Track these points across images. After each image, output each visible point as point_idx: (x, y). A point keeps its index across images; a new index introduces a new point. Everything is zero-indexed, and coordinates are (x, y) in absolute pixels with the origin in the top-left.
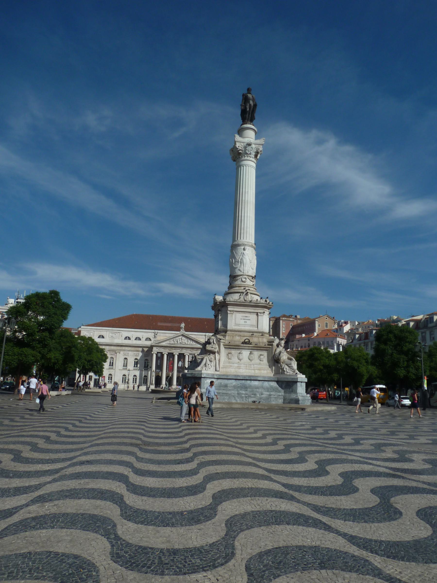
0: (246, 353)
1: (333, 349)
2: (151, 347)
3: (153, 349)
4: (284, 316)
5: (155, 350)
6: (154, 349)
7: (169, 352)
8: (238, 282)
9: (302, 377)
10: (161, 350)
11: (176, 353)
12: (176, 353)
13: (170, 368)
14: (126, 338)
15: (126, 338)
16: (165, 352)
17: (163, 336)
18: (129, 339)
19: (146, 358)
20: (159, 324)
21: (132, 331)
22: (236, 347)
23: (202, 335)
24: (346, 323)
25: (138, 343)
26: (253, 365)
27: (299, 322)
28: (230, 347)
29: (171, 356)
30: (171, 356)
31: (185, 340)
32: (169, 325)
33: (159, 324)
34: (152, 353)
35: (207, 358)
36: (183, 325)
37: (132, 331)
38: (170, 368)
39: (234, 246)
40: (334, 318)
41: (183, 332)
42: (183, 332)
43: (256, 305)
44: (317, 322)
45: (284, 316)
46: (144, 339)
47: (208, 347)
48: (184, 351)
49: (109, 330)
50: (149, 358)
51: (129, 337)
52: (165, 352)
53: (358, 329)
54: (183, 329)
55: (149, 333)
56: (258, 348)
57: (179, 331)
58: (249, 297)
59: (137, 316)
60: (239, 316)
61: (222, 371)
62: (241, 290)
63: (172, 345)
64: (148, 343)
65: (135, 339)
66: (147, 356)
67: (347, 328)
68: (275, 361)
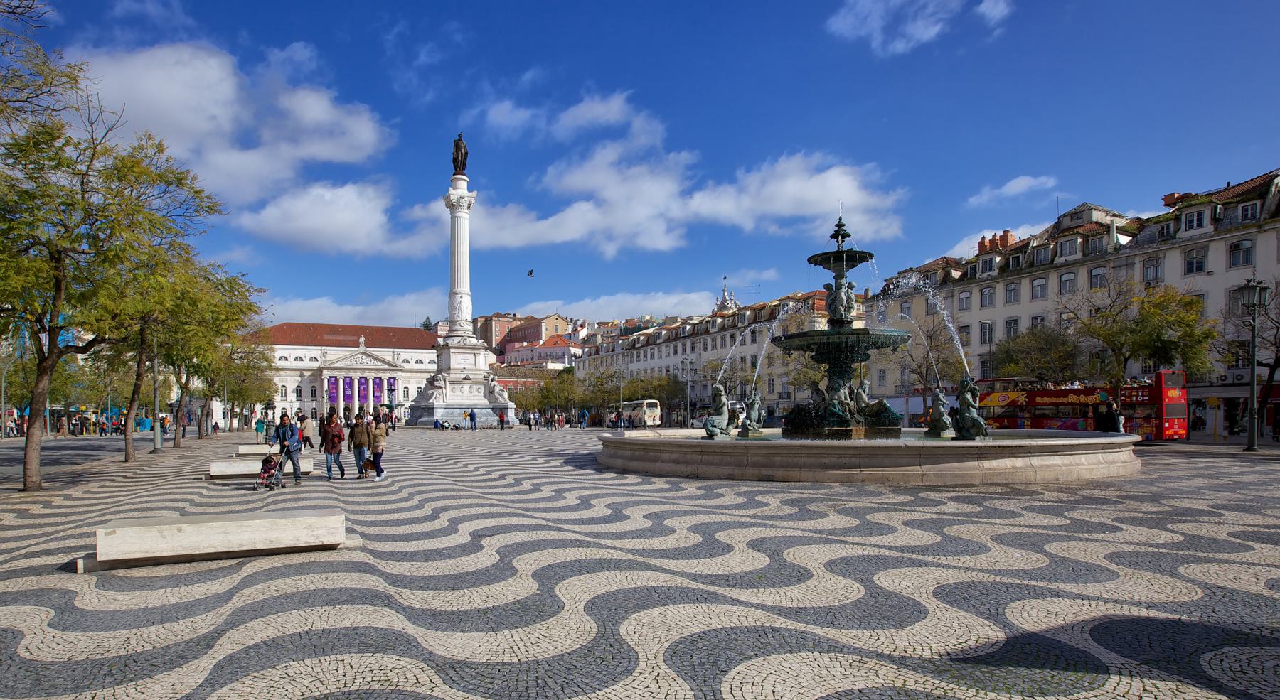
0: (466, 387)
2: (320, 370)
4: (498, 315)
5: (326, 374)
6: (325, 372)
8: (457, 327)
9: (512, 405)
10: (335, 374)
11: (356, 376)
12: (356, 376)
13: (348, 398)
15: (281, 359)
17: (336, 356)
20: (326, 337)
22: (459, 383)
24: (582, 326)
25: (299, 364)
26: (474, 398)
27: (519, 323)
28: (452, 383)
29: (349, 383)
30: (349, 383)
32: (341, 338)
33: (326, 337)
35: (436, 392)
36: (362, 339)
38: (348, 398)
39: (452, 294)
41: (362, 348)
42: (362, 348)
43: (474, 347)
45: (498, 315)
47: (436, 384)
48: (365, 374)
53: (596, 335)
55: (315, 351)
56: (477, 383)
57: (357, 345)
58: (467, 342)
59: (289, 325)
60: (460, 356)
61: (449, 401)
62: (461, 333)
64: (315, 365)
67: (583, 333)
68: (490, 393)
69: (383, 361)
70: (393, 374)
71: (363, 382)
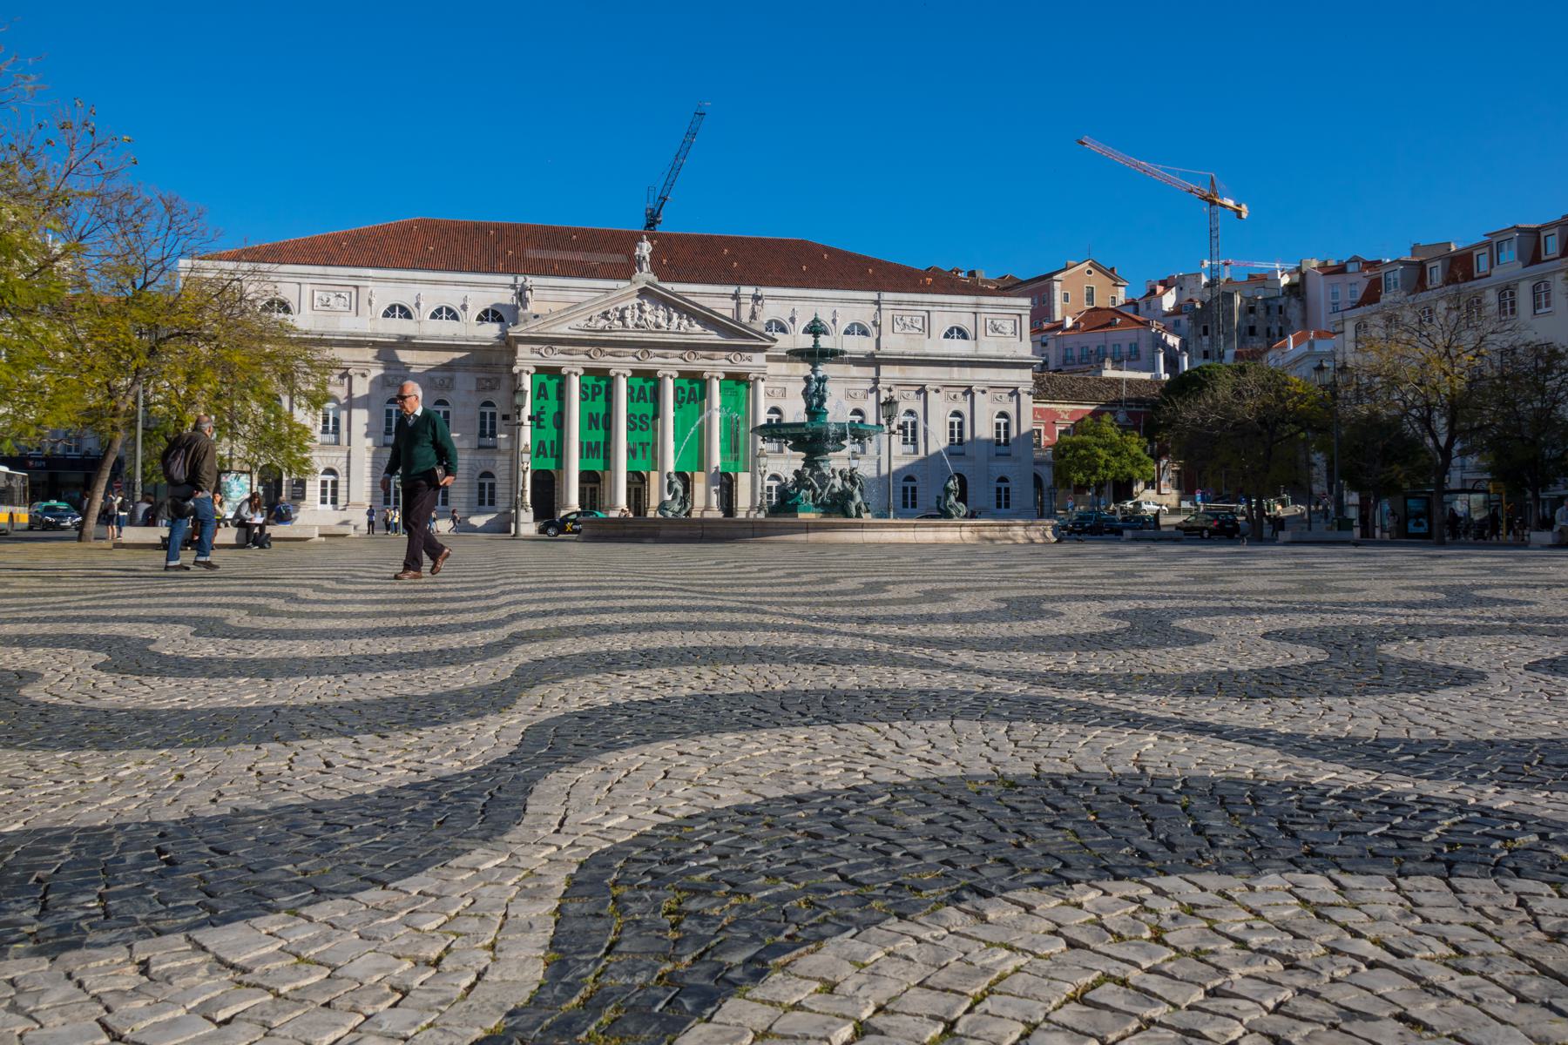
1: (1152, 367)
3: (514, 352)
5: (527, 359)
6: (523, 351)
7: (590, 365)
10: (555, 358)
12: (621, 366)
14: (390, 312)
15: (390, 312)
16: (574, 364)
18: (406, 314)
19: (487, 396)
20: (531, 254)
21: (415, 281)
23: (723, 295)
29: (600, 383)
30: (600, 383)
31: (655, 315)
34: (516, 370)
37: (415, 281)
40: (1112, 270)
41: (645, 276)
44: (1057, 285)
46: (474, 311)
48: (653, 362)
49: (309, 275)
50: (499, 397)
51: (402, 309)
52: (574, 364)
54: (646, 267)
57: (625, 271)
63: (604, 337)
65: (433, 316)
66: (492, 389)
69: (708, 320)
70: (741, 364)
71: (648, 385)
